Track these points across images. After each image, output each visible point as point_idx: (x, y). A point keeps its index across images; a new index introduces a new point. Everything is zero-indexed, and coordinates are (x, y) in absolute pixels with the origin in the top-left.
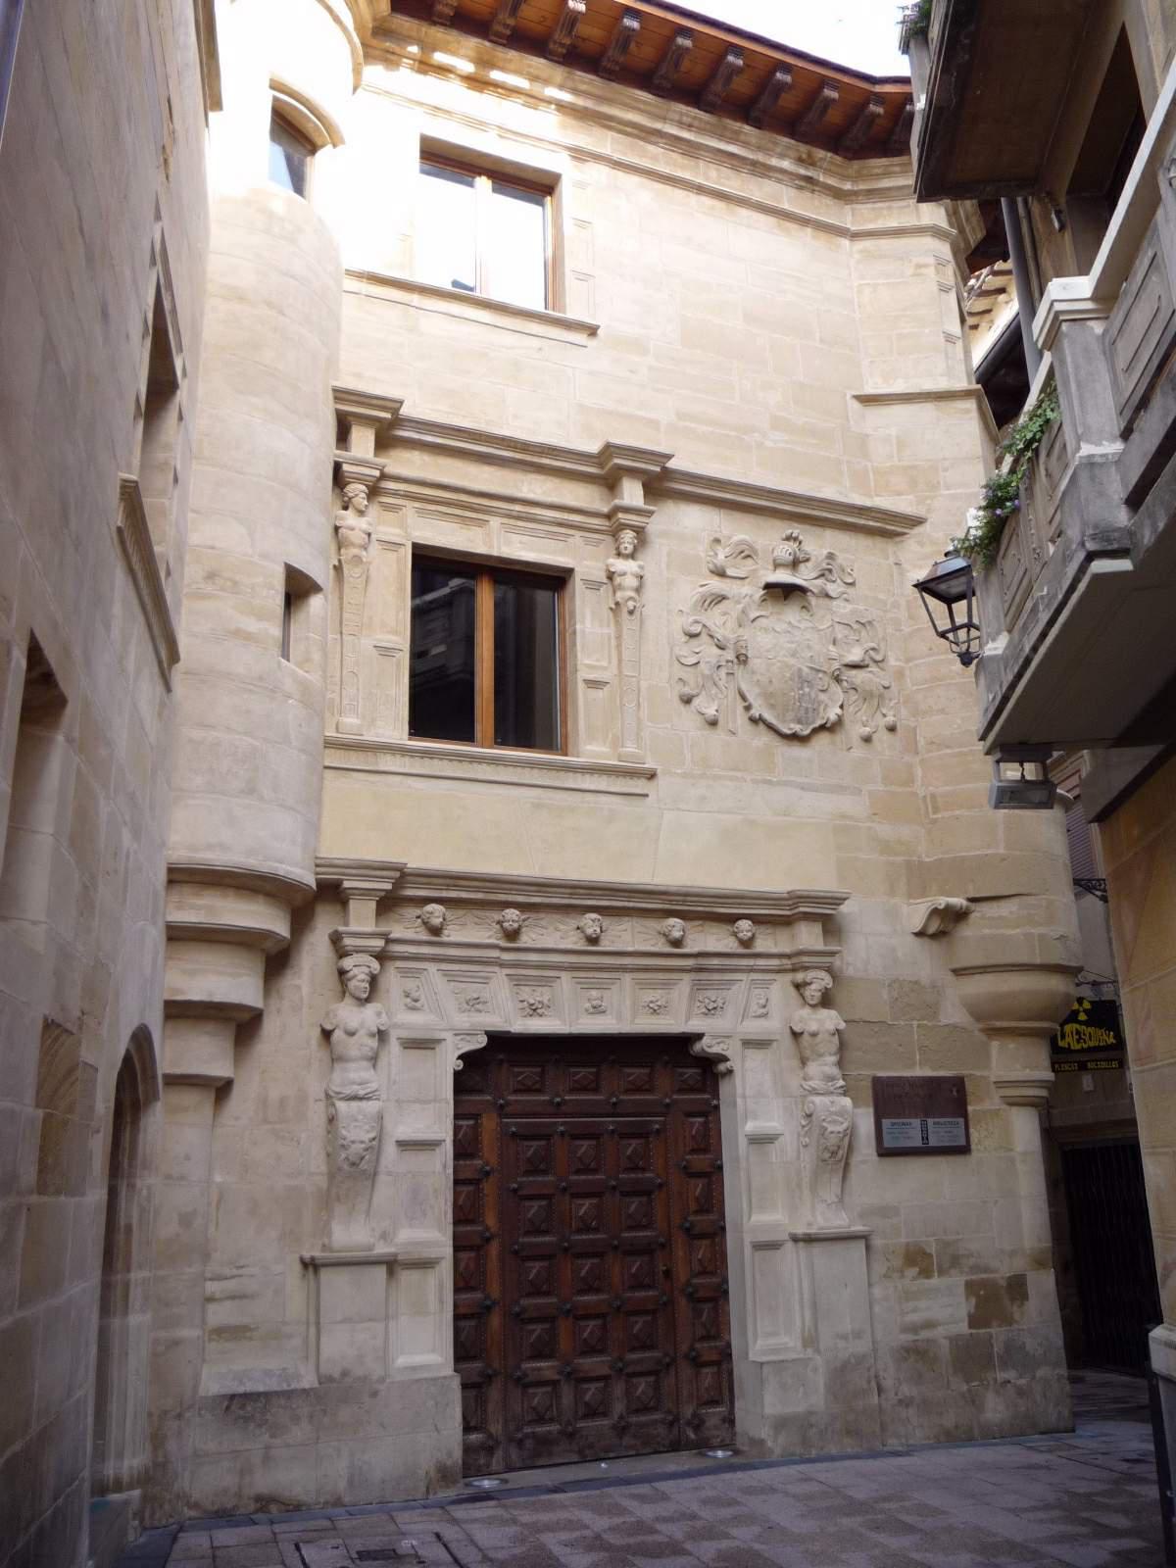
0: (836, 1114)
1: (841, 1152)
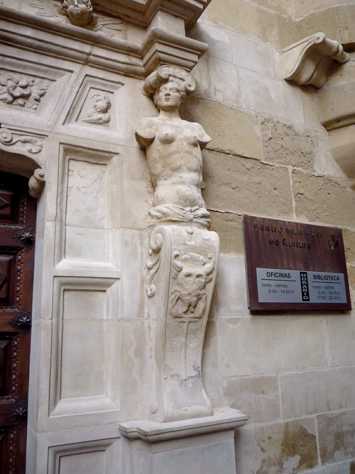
0: (193, 249)
1: (201, 305)
